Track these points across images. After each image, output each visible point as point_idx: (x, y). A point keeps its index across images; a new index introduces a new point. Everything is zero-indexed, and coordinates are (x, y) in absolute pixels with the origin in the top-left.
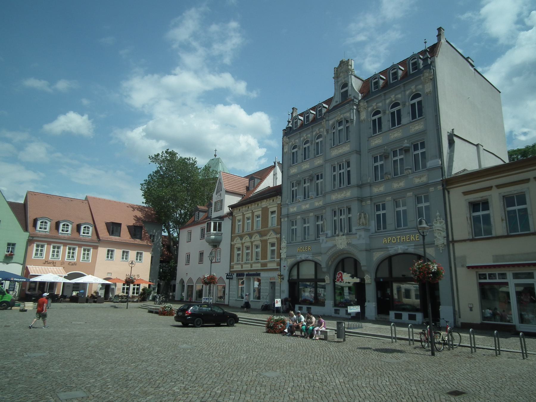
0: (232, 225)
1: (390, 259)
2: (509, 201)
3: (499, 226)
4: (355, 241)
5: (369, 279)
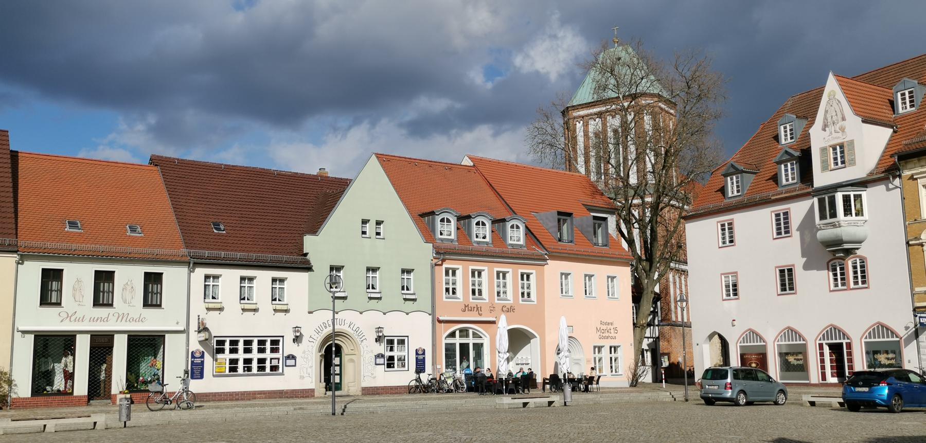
0: (903, 199)
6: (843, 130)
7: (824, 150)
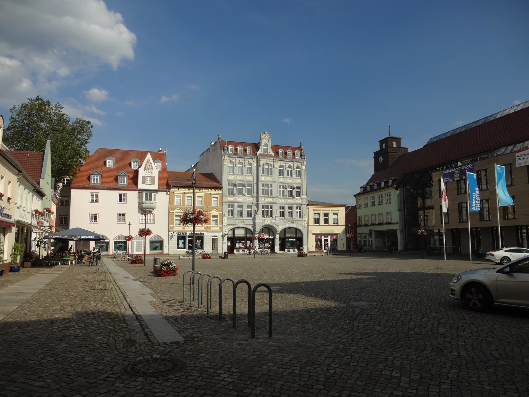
1: (285, 229)
2: (325, 215)
3: (322, 222)
4: (274, 221)
5: (277, 237)
6: (152, 172)
7: (143, 178)
